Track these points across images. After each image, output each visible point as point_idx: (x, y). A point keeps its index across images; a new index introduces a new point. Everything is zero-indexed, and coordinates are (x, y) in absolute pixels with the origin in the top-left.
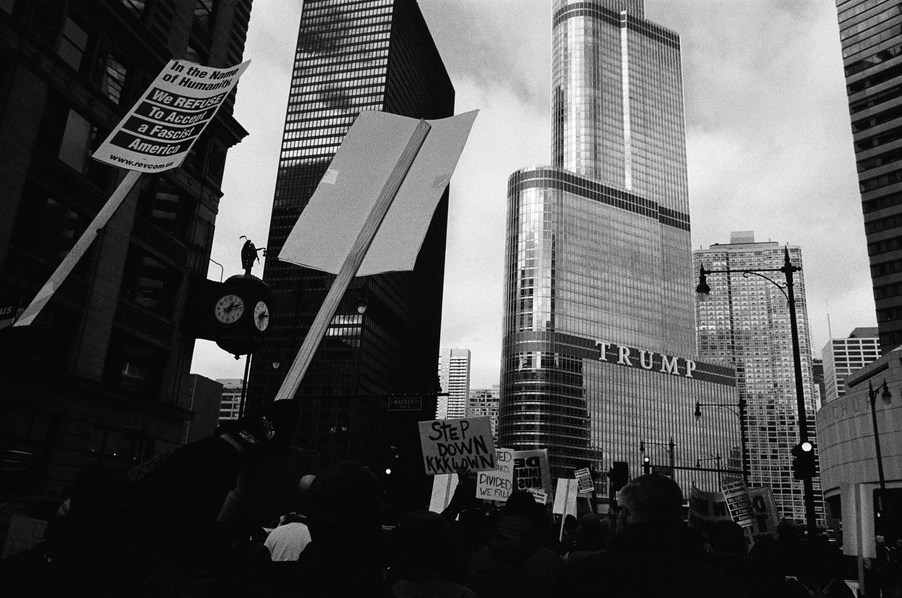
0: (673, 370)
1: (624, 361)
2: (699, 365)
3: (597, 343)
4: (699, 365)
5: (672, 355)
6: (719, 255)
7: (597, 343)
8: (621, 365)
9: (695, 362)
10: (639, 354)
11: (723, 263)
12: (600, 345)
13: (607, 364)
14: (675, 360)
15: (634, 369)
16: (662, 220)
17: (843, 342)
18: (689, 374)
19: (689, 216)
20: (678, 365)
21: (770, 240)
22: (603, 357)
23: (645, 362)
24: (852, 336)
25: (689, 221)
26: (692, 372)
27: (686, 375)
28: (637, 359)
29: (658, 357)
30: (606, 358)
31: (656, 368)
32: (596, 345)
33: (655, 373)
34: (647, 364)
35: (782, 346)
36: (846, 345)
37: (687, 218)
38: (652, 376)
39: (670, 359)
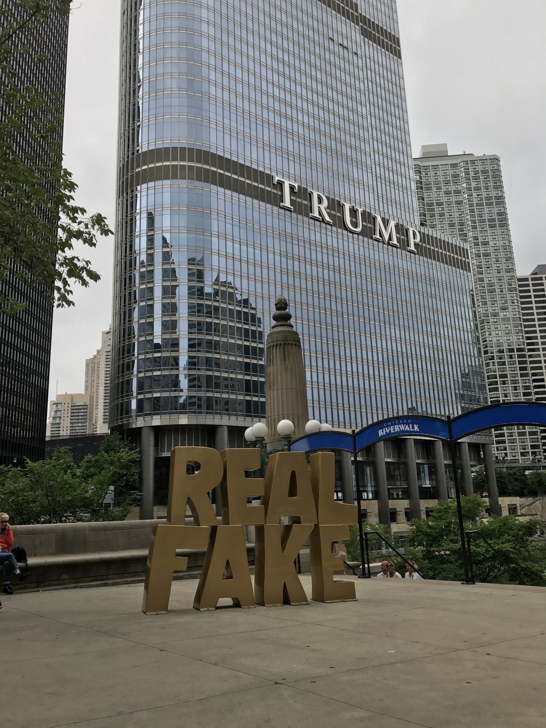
0: (390, 238)
1: (320, 213)
2: (424, 237)
3: (277, 178)
4: (424, 237)
5: (387, 217)
7: (277, 178)
9: (420, 232)
10: (341, 207)
12: (281, 184)
13: (294, 215)
14: (392, 224)
15: (334, 229)
16: (365, 33)
17: (527, 279)
18: (412, 248)
19: (398, 39)
20: (397, 232)
21: (464, 152)
23: (351, 222)
24: (533, 274)
25: (399, 46)
26: (416, 245)
29: (369, 218)
33: (366, 239)
34: (355, 225)
35: (485, 266)
36: (530, 282)
37: (397, 41)
38: (361, 244)
39: (386, 222)
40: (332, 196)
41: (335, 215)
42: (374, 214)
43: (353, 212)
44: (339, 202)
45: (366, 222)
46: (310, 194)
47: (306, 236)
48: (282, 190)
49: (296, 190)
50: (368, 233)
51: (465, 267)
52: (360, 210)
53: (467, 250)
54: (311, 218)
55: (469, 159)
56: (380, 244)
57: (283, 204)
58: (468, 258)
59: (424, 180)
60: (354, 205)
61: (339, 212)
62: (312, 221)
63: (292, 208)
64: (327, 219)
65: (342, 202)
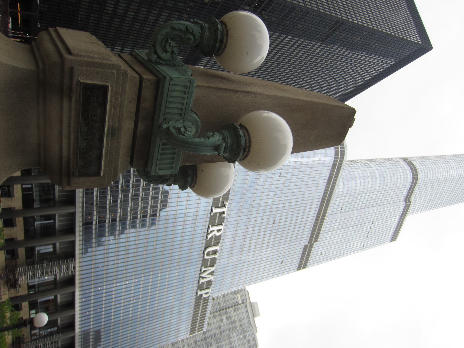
0: (203, 278)
1: (212, 231)
2: (206, 300)
4: (206, 300)
6: (244, 297)
8: (208, 229)
9: (209, 297)
10: (217, 244)
11: (240, 301)
12: (224, 206)
13: (209, 216)
14: (211, 278)
15: (204, 241)
18: (200, 293)
22: (215, 211)
23: (209, 252)
26: (201, 295)
27: (199, 291)
28: (213, 243)
30: (214, 213)
31: (205, 263)
32: (225, 203)
33: (201, 262)
34: (208, 254)
37: (305, 267)
39: (212, 273)
40: (222, 238)
41: (212, 241)
42: (215, 265)
43: (215, 252)
44: (219, 243)
45: (211, 261)
46: (221, 224)
47: (199, 224)
48: (221, 207)
49: (223, 216)
50: (205, 263)
51: (193, 330)
52: (216, 256)
53: (202, 330)
54: (208, 226)
55: (254, 330)
56: (199, 272)
57: (214, 208)
58: (198, 332)
59: (239, 306)
60: (219, 252)
61: (214, 243)
62: (207, 227)
63: (213, 214)
64: (210, 236)
65: (220, 245)
